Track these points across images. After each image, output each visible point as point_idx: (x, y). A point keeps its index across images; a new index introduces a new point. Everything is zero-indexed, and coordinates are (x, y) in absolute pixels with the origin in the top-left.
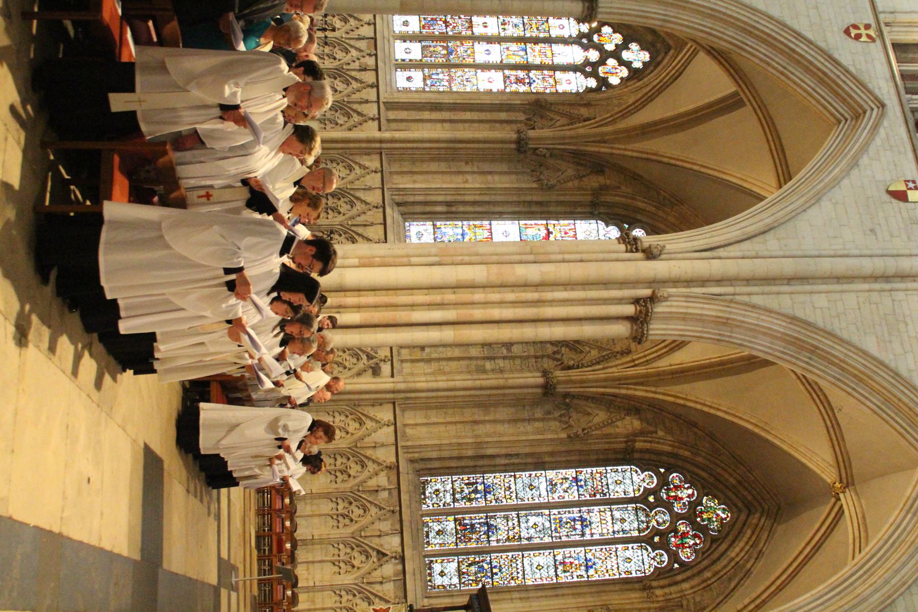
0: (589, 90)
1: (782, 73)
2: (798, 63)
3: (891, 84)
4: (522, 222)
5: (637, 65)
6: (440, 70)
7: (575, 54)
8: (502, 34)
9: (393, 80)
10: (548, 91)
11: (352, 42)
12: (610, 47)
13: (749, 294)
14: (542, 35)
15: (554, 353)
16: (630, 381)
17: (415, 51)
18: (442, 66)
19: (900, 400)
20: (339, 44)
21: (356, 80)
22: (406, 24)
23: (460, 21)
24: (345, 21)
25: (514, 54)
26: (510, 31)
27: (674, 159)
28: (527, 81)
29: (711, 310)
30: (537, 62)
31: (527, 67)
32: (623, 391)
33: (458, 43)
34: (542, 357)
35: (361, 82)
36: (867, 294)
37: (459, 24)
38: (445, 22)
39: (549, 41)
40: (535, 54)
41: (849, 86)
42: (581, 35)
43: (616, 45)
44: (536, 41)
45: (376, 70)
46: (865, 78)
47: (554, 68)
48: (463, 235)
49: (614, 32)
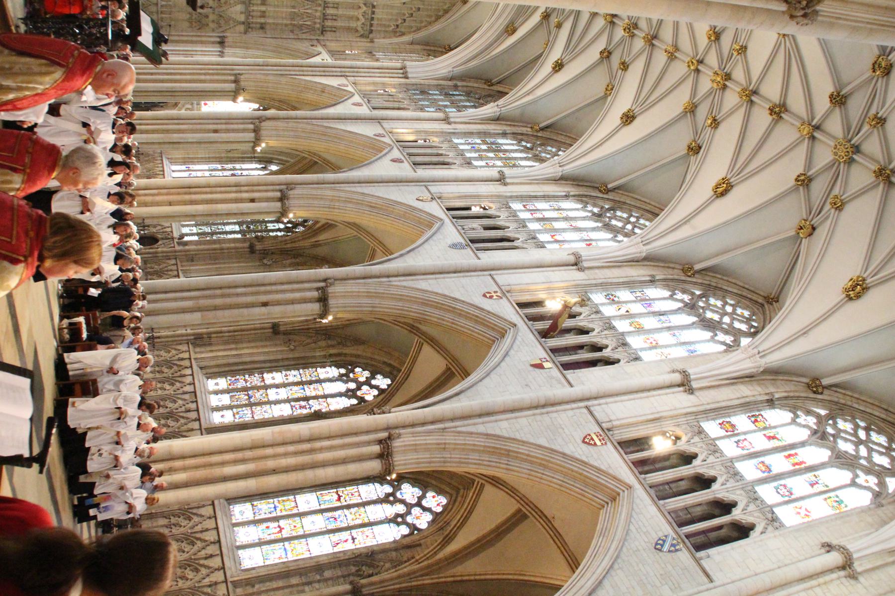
0: (352, 405)
1: (453, 323)
2: (460, 315)
3: (518, 316)
4: (318, 493)
5: (384, 386)
6: (244, 409)
7: (341, 387)
8: (286, 382)
9: (211, 418)
10: (324, 410)
11: (179, 396)
12: (362, 379)
13: (456, 427)
14: (314, 379)
15: (357, 571)
16: (417, 574)
17: (226, 399)
18: (246, 405)
19: (572, 471)
20: (169, 399)
21: (183, 417)
22: (217, 384)
23: (255, 378)
24: (173, 384)
25: (297, 392)
26: (291, 379)
27: (484, 575)
28: (308, 406)
29: (431, 440)
30: (313, 394)
31: (307, 399)
32: (414, 583)
33: (256, 391)
34: (349, 575)
35: (187, 418)
36: (533, 417)
37: (255, 380)
38: (245, 380)
39: (319, 381)
40: (310, 391)
41: (494, 320)
42: (341, 375)
43: (367, 378)
44: (310, 383)
45: (198, 410)
46: (502, 315)
47: (325, 397)
48: (275, 507)
49: (364, 370)
